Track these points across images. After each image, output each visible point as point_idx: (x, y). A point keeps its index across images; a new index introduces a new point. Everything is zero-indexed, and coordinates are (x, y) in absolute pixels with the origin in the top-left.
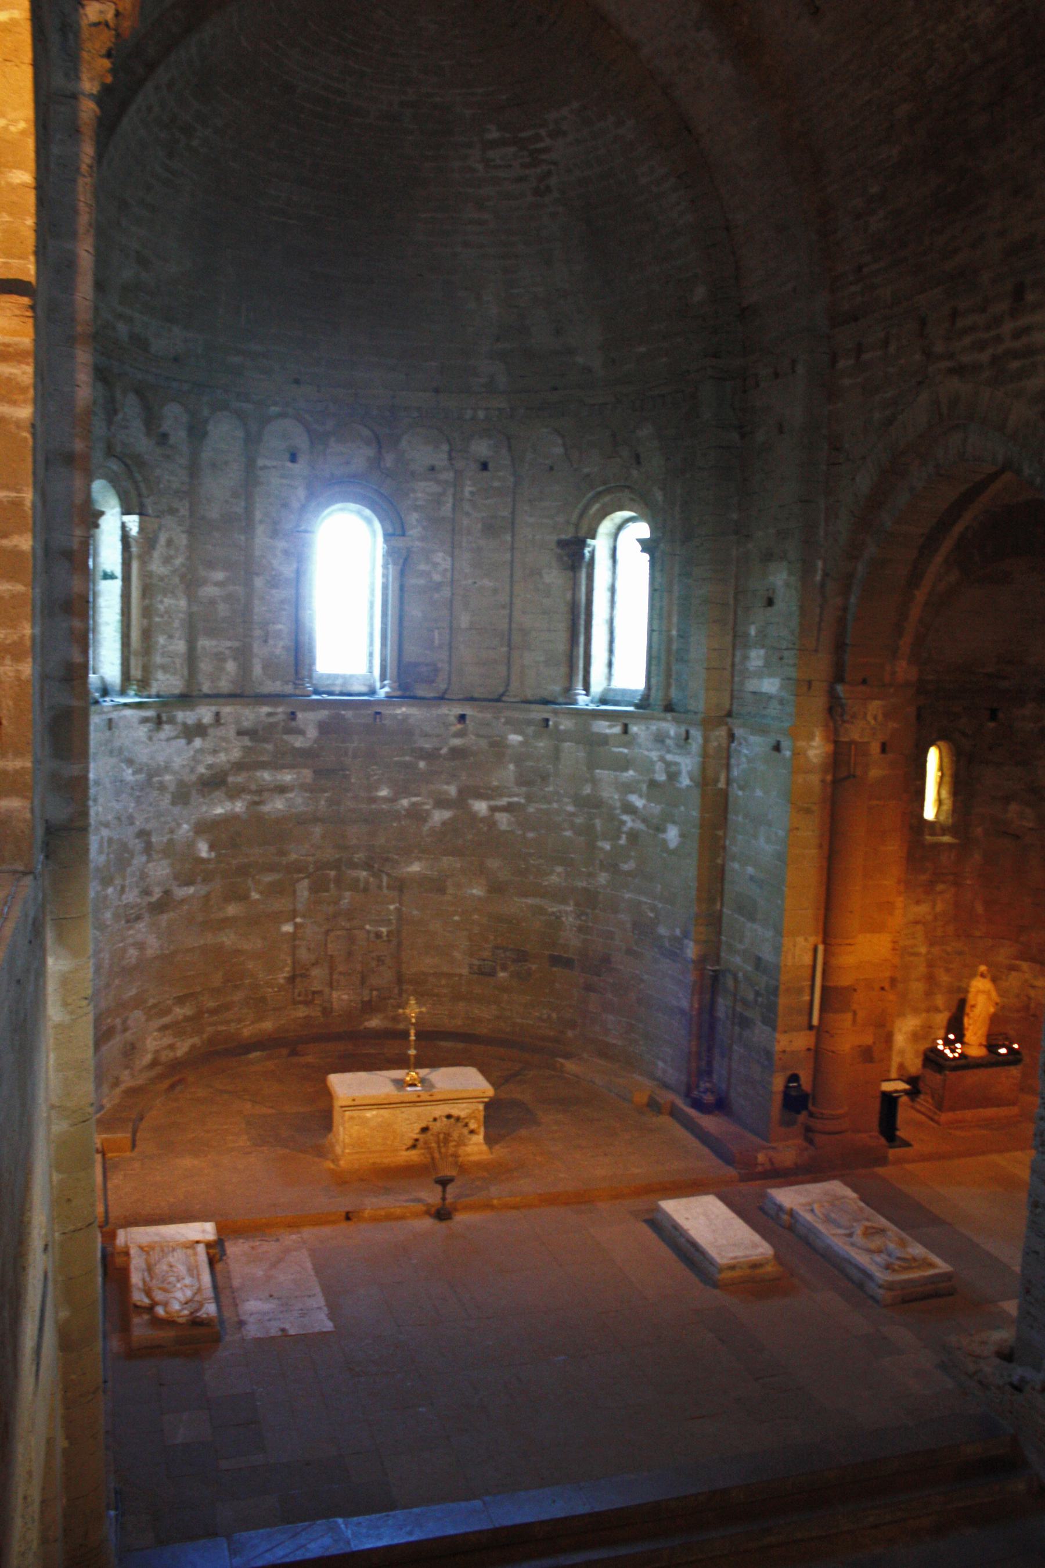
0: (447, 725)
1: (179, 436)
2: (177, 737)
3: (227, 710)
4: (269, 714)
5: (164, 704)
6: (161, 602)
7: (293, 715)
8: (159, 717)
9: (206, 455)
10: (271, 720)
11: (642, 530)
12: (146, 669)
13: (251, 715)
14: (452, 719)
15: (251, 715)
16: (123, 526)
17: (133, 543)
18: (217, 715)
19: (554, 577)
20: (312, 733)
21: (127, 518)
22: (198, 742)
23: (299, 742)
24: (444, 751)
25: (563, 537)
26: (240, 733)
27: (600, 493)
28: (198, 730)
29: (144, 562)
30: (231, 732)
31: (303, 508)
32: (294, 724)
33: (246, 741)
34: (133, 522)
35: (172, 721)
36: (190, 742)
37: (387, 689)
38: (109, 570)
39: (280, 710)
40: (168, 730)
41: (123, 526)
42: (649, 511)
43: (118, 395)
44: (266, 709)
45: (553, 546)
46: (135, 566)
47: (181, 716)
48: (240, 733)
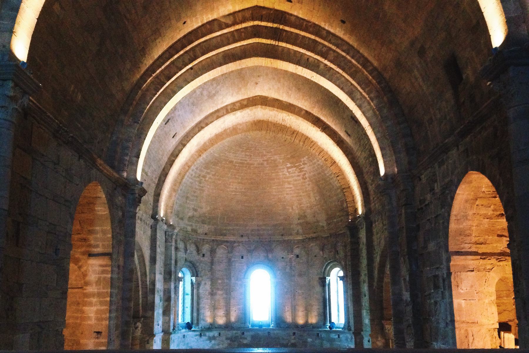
0: (290, 336)
1: (208, 254)
2: (206, 340)
3: (222, 332)
4: (236, 333)
5: (202, 330)
6: (203, 301)
7: (243, 333)
8: (201, 334)
9: (215, 259)
10: (237, 335)
11: (341, 274)
12: (198, 320)
13: (230, 334)
14: (292, 334)
15: (230, 334)
16: (191, 280)
17: (194, 285)
18: (220, 334)
19: (318, 289)
20: (249, 339)
21: (192, 278)
22: (213, 342)
23: (245, 342)
24: (290, 344)
25: (320, 276)
26: (227, 339)
27: (329, 263)
28: (214, 338)
29: (198, 290)
30: (224, 338)
31: (246, 272)
32: (243, 336)
33: (229, 341)
34: (194, 279)
35: (205, 335)
36: (210, 342)
37: (273, 325)
38: (188, 293)
39: (239, 332)
40: (204, 338)
41: (191, 280)
42: (344, 269)
43: (188, 247)
44: (235, 332)
45: (318, 279)
46: (195, 291)
47: (208, 334)
48: (227, 339)
